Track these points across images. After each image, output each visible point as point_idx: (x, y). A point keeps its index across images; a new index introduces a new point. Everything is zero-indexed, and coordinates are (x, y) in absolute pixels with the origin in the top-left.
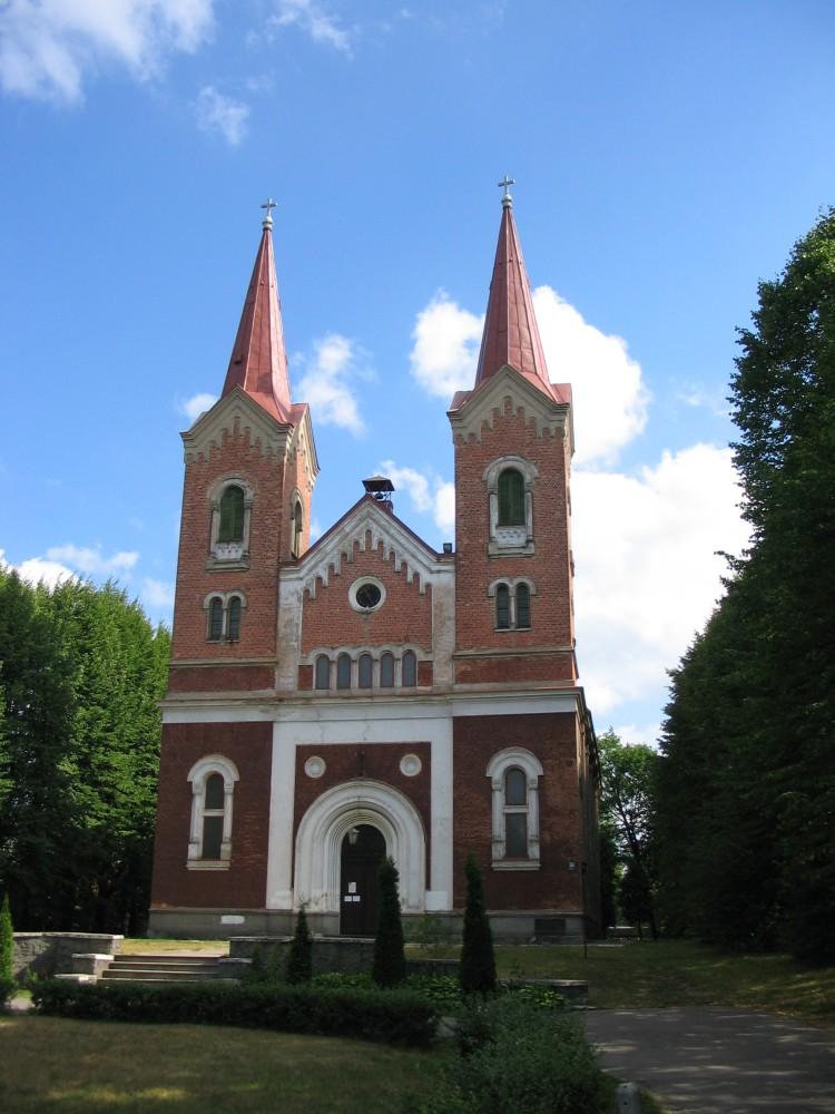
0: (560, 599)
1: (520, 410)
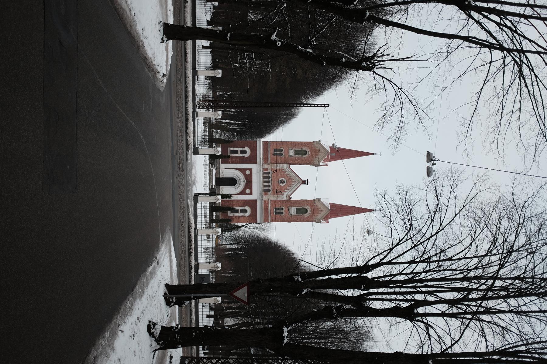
1: (320, 213)
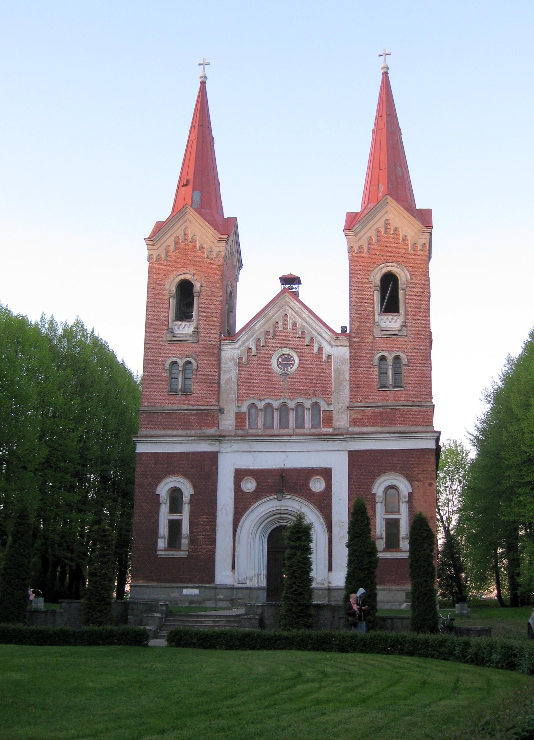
0: (425, 368)
1: (396, 230)
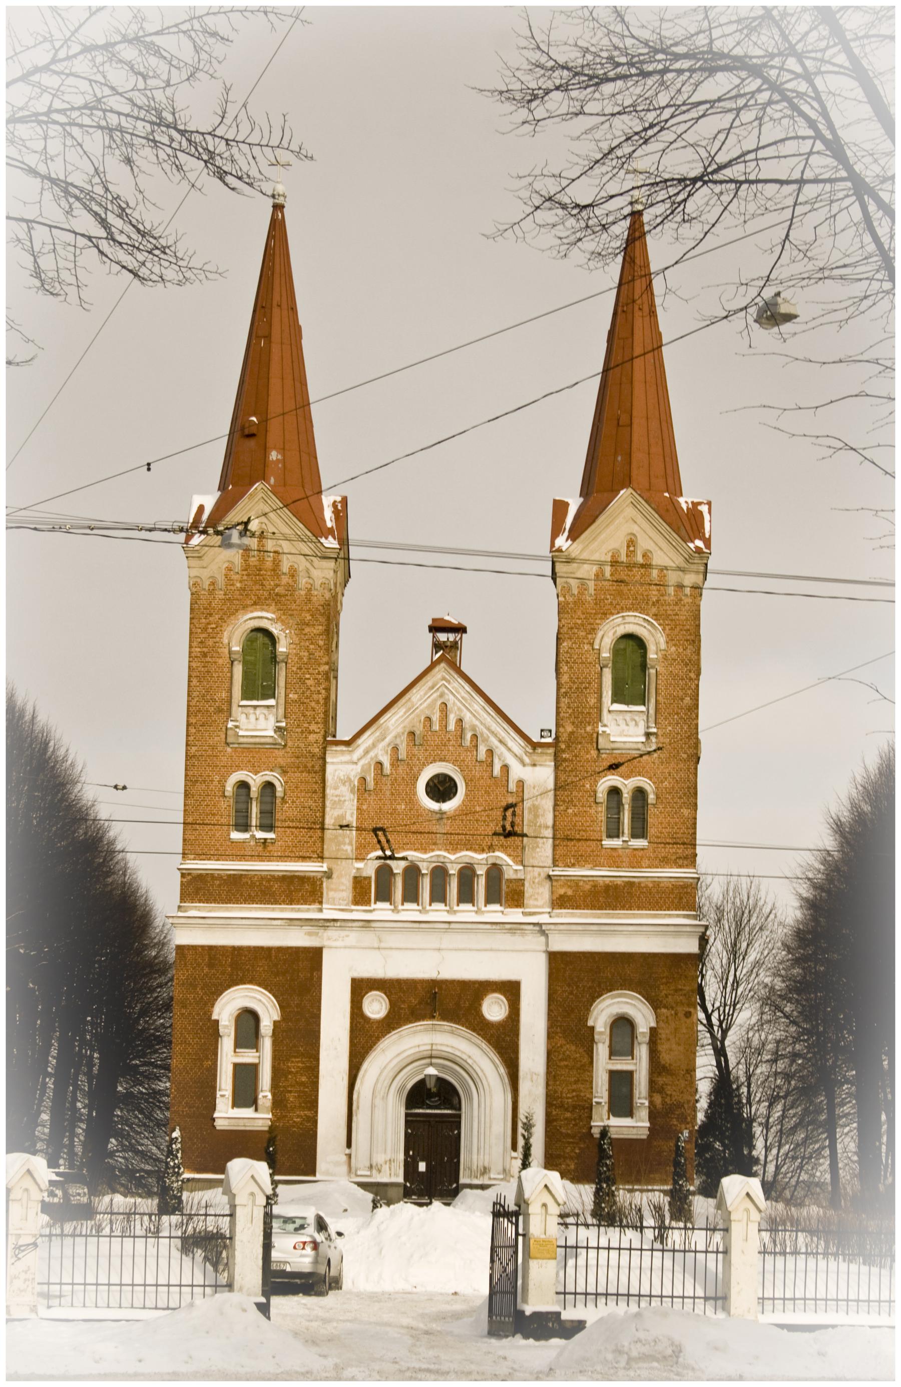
0: (686, 812)
